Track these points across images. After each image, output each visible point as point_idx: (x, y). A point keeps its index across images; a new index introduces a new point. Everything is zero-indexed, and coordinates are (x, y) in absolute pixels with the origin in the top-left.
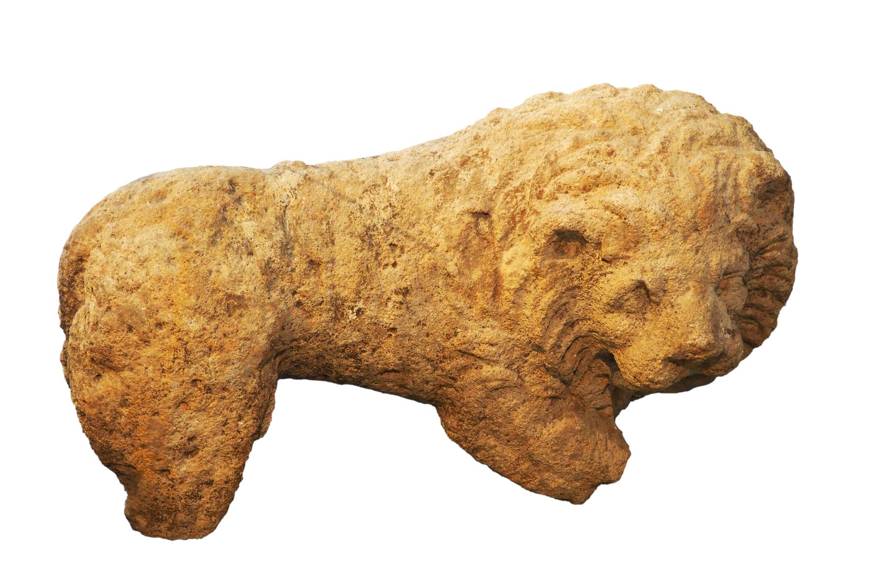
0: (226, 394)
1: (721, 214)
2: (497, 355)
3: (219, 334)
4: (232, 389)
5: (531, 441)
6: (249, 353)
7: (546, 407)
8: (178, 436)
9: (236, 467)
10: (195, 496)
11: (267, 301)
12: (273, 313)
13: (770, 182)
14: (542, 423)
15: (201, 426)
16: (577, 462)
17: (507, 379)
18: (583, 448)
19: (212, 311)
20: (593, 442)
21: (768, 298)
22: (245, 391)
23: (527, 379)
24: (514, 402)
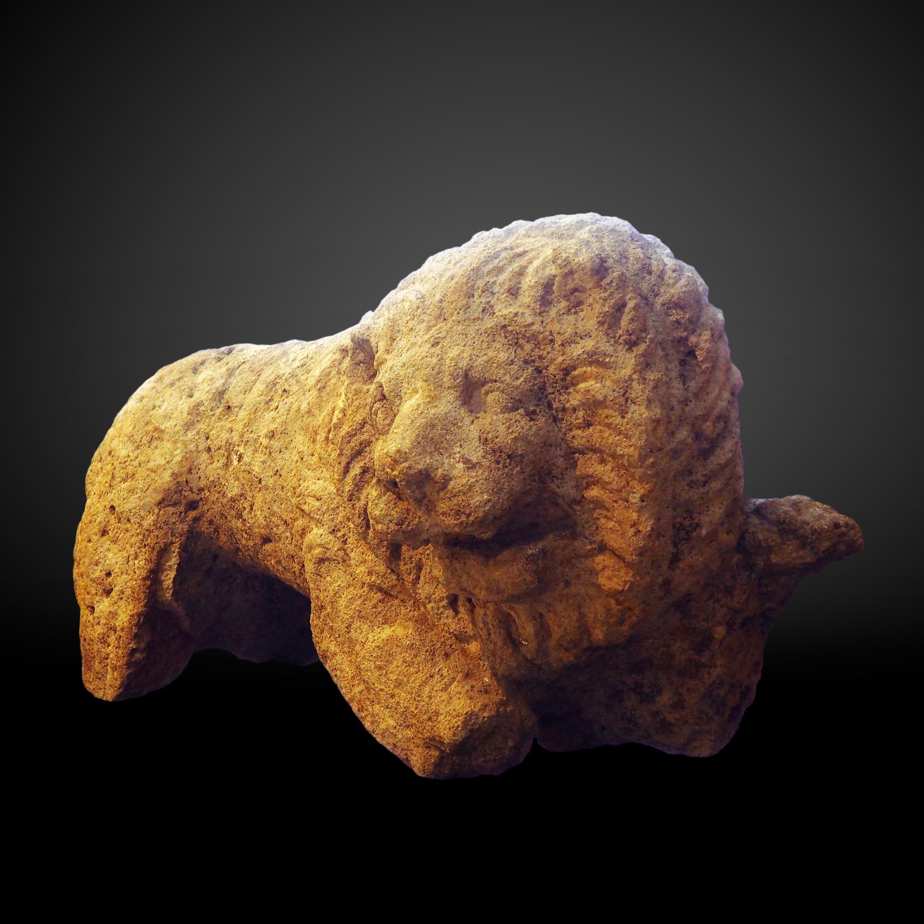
0: (129, 526)
1: (478, 301)
2: (319, 512)
3: (136, 463)
4: (132, 521)
5: (358, 648)
6: (150, 485)
7: (374, 602)
8: (100, 567)
9: (130, 614)
10: (104, 640)
11: (181, 438)
12: (182, 451)
13: (571, 273)
14: (370, 624)
15: (113, 560)
16: (403, 694)
17: (327, 546)
18: (410, 675)
19: (138, 440)
20: (426, 671)
21: (609, 467)
22: (140, 525)
23: (352, 555)
24: (339, 582)
